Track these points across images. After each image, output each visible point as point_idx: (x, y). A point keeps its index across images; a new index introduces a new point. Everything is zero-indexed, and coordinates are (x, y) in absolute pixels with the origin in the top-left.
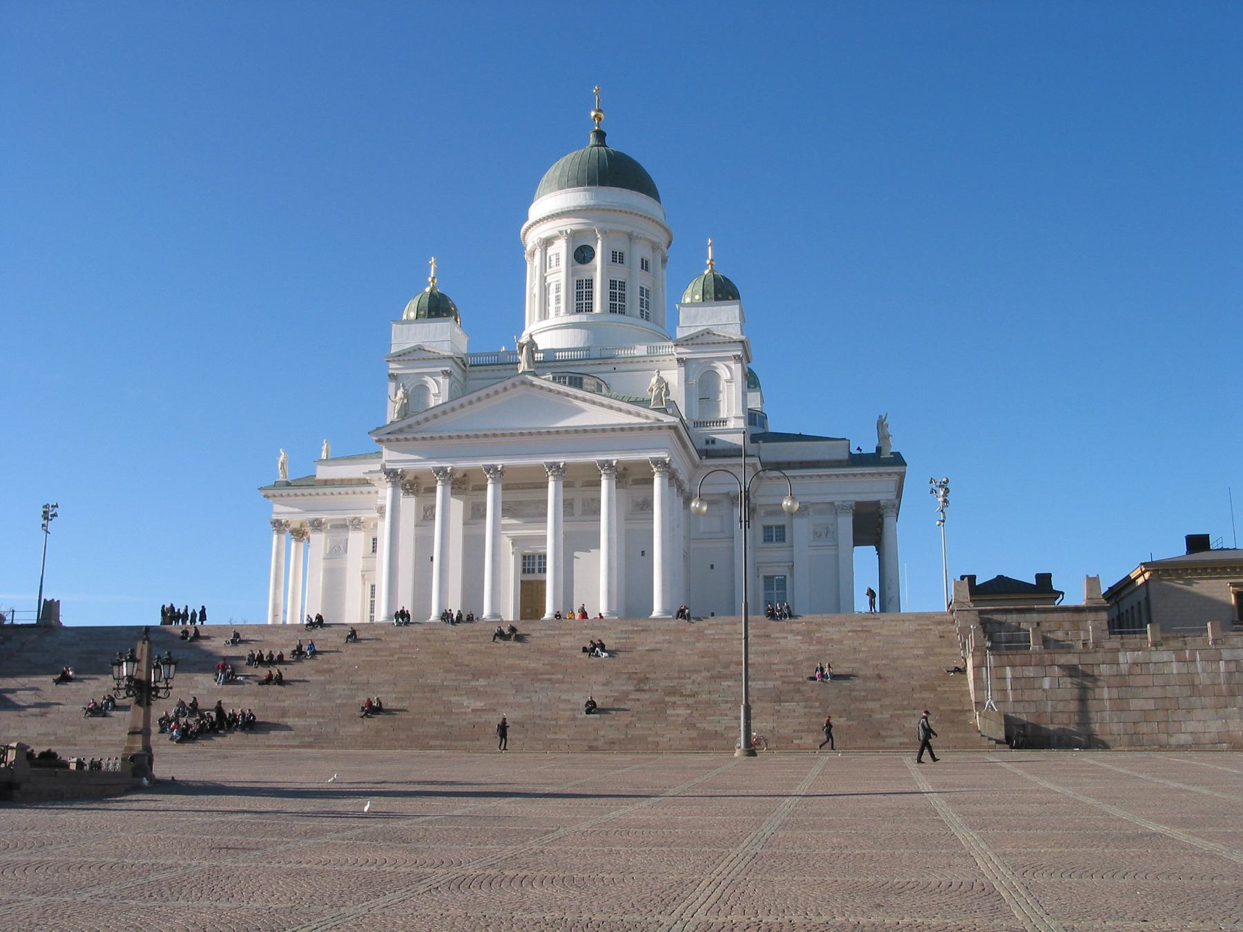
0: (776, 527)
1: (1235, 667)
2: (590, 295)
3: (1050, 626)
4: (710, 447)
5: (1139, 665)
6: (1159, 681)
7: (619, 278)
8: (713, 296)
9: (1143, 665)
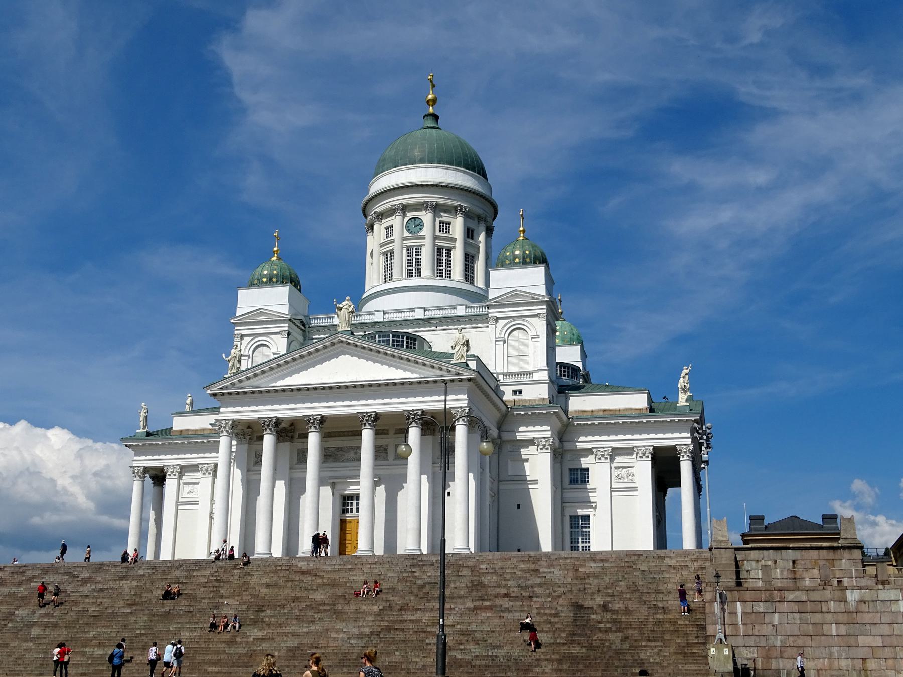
2: (419, 262)
3: (805, 564)
4: (518, 397)
5: (867, 603)
6: (886, 618)
8: (521, 261)
9: (871, 603)
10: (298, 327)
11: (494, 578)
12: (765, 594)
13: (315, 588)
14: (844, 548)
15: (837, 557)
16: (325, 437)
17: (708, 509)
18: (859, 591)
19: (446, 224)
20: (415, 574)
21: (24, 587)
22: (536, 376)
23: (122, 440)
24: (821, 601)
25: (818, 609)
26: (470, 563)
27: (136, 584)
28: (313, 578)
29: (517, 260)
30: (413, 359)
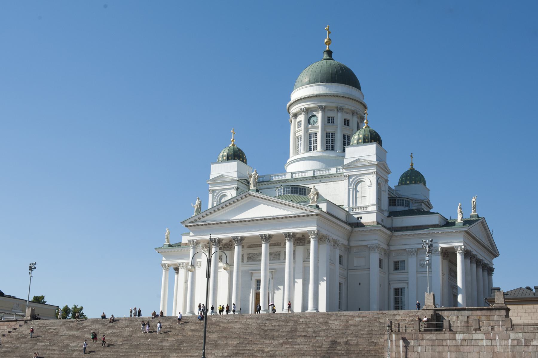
0: (401, 261)
1: (517, 342)
2: (316, 142)
5: (466, 341)
6: (476, 349)
7: (330, 130)
8: (363, 141)
9: (468, 341)
10: (246, 185)
11: (304, 326)
12: (414, 336)
13: (214, 332)
14: (496, 309)
15: (492, 314)
16: (248, 248)
17: (428, 287)
18: (462, 334)
19: (332, 118)
20: (266, 325)
21: (80, 331)
22: (370, 209)
23: (156, 249)
24: (443, 340)
25: (441, 344)
26: (296, 319)
27: (132, 330)
28: (216, 327)
29: (360, 141)
30: (287, 204)
